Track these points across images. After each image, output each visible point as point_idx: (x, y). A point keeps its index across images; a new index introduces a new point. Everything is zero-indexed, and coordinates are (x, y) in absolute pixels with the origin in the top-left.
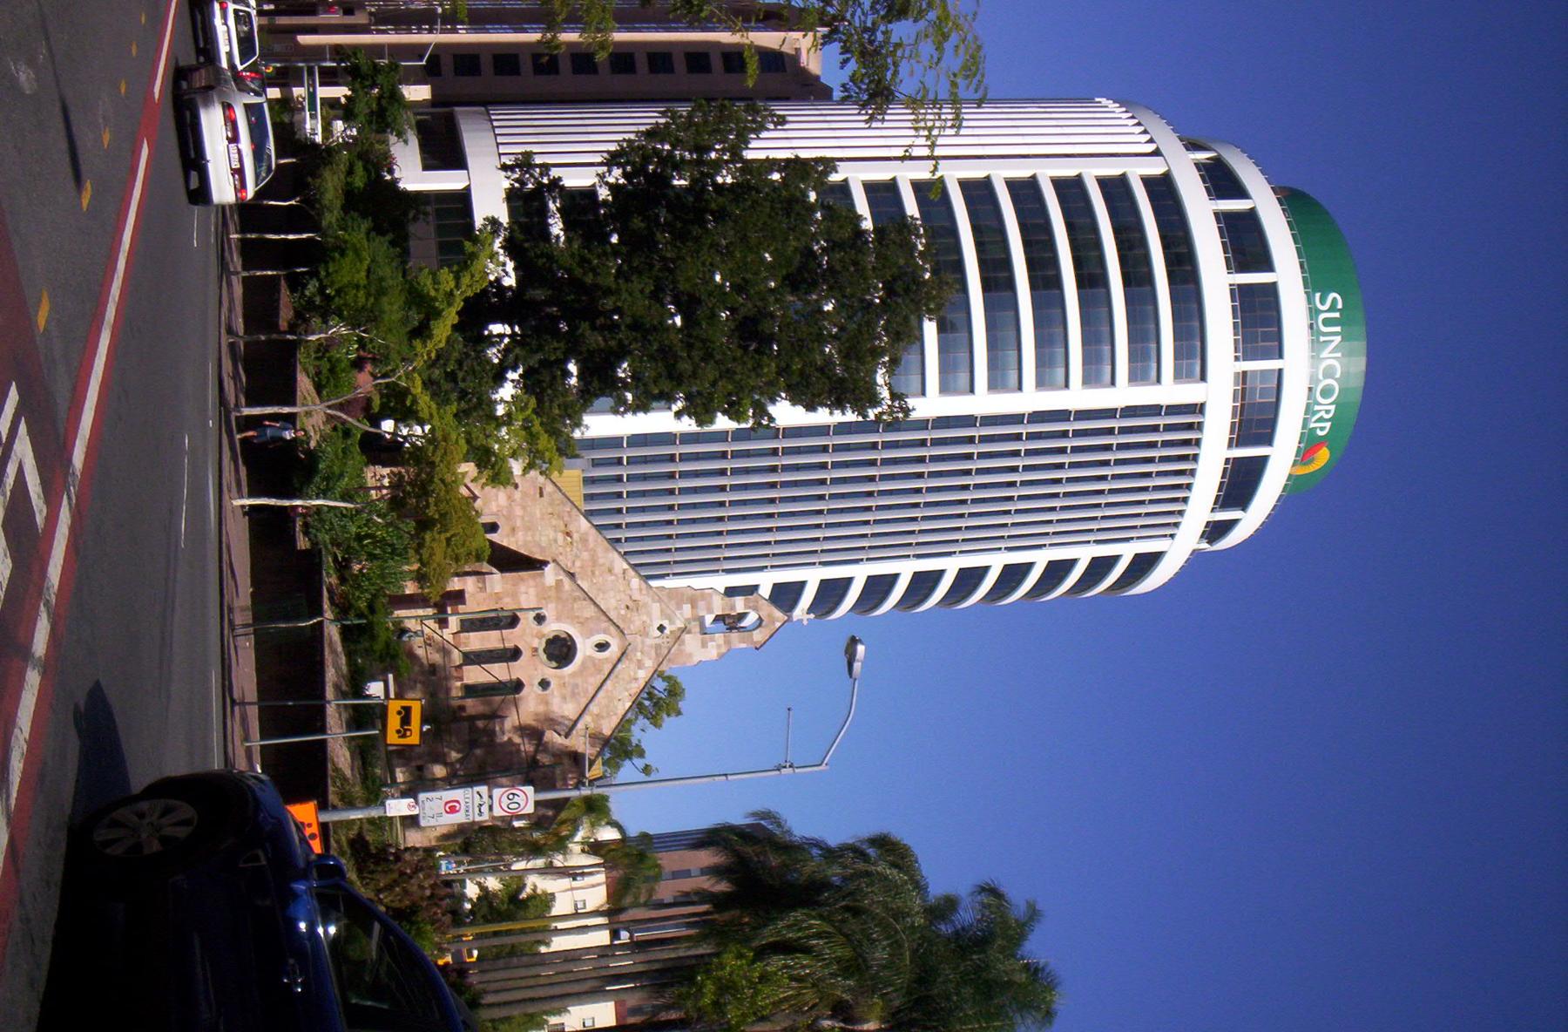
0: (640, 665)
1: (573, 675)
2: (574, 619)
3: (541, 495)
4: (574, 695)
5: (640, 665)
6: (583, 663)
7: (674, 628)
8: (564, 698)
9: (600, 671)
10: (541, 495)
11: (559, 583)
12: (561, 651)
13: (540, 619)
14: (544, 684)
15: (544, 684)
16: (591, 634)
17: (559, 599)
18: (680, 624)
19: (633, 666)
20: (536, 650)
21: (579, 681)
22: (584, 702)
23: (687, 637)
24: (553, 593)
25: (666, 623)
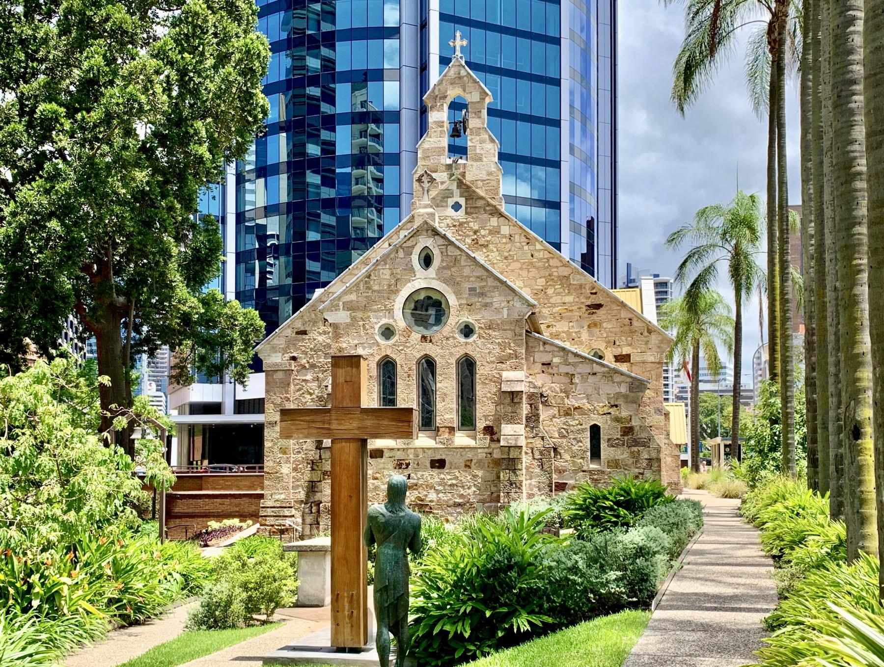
0: (495, 232)
1: (458, 294)
2: (393, 291)
3: (304, 333)
4: (482, 294)
5: (495, 232)
6: (445, 281)
7: (456, 192)
8: (486, 305)
9: (456, 260)
10: (304, 333)
11: (350, 307)
12: (428, 309)
13: (388, 332)
14: (467, 331)
15: (467, 331)
16: (412, 270)
17: (365, 308)
18: (454, 187)
19: (495, 239)
20: (424, 338)
21: (467, 285)
22: (491, 282)
23: (469, 178)
24: (359, 315)
25: (451, 202)
